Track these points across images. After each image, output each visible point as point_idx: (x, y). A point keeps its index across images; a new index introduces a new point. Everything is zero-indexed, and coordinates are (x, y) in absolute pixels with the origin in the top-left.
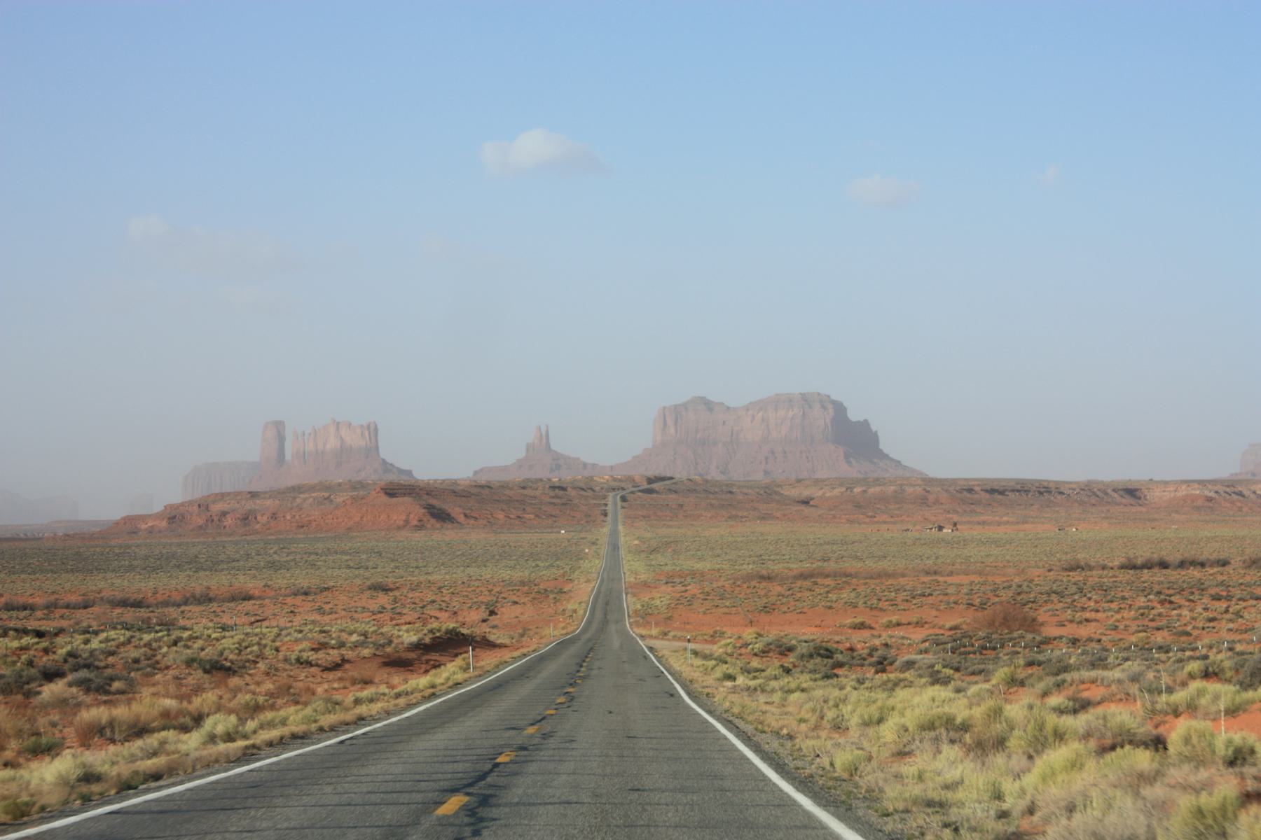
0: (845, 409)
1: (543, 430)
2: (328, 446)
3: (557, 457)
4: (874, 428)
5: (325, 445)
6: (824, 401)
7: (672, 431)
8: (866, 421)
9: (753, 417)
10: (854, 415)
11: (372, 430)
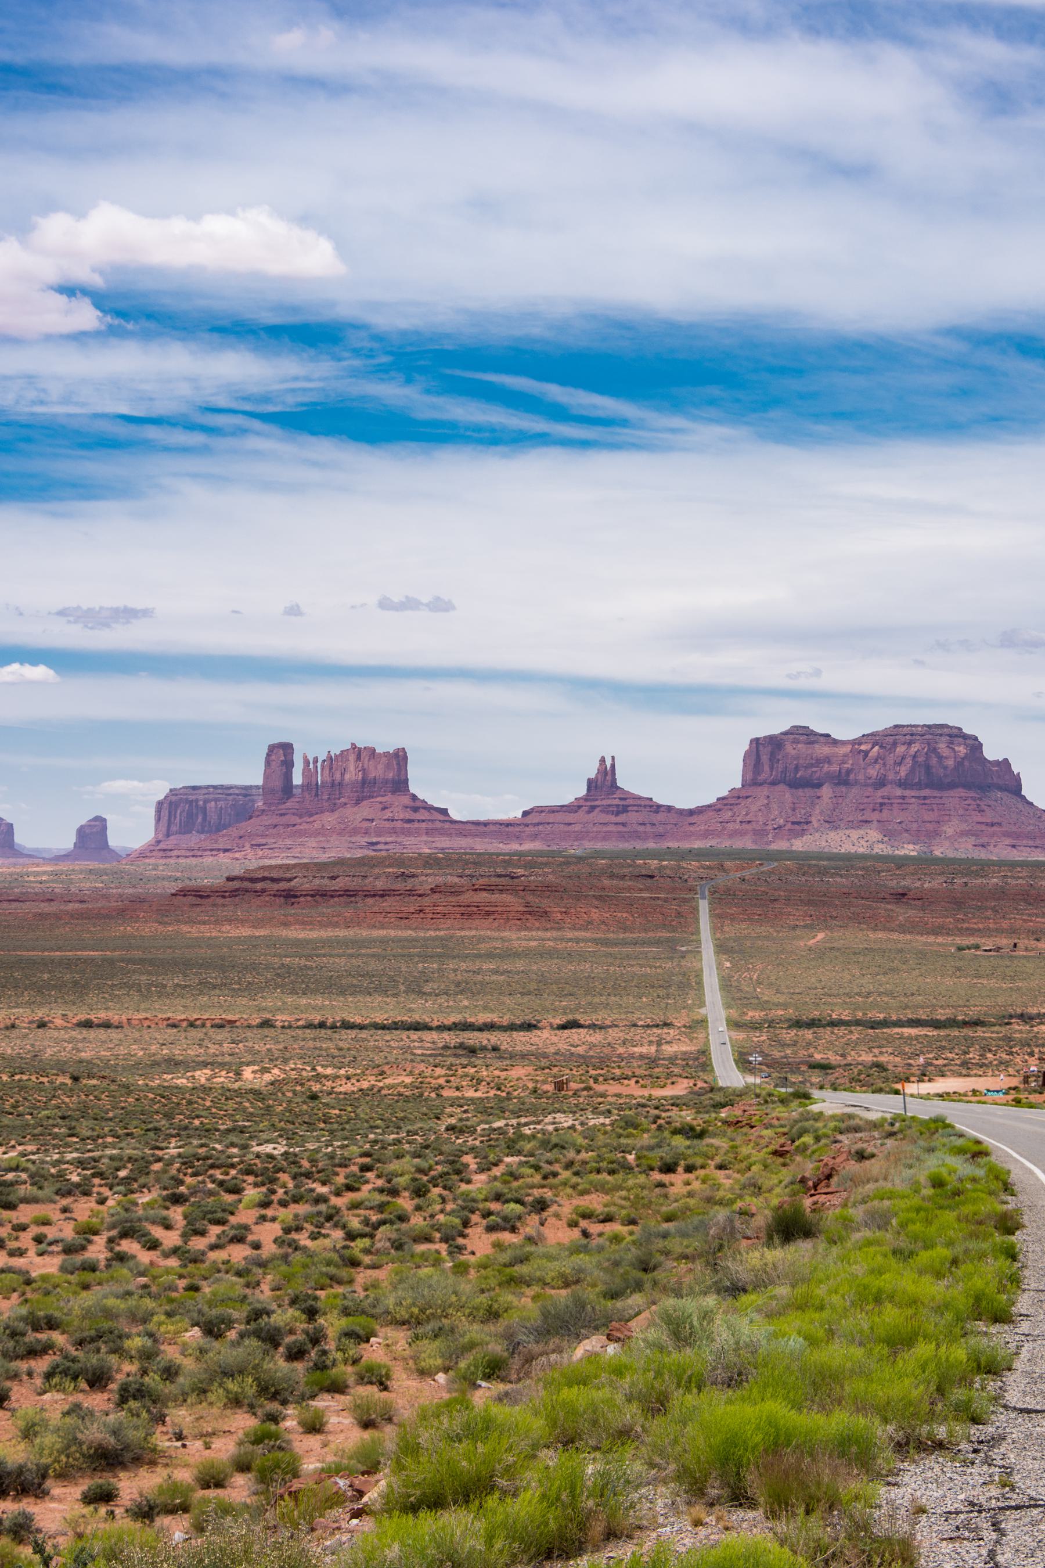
0: (982, 745)
1: (608, 763)
2: (347, 777)
3: (626, 796)
4: (1015, 769)
5: (343, 775)
6: (956, 735)
7: (767, 768)
8: (1006, 760)
9: (866, 753)
10: (991, 753)
11: (400, 758)
